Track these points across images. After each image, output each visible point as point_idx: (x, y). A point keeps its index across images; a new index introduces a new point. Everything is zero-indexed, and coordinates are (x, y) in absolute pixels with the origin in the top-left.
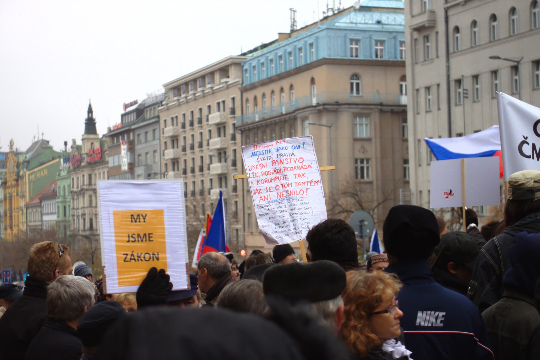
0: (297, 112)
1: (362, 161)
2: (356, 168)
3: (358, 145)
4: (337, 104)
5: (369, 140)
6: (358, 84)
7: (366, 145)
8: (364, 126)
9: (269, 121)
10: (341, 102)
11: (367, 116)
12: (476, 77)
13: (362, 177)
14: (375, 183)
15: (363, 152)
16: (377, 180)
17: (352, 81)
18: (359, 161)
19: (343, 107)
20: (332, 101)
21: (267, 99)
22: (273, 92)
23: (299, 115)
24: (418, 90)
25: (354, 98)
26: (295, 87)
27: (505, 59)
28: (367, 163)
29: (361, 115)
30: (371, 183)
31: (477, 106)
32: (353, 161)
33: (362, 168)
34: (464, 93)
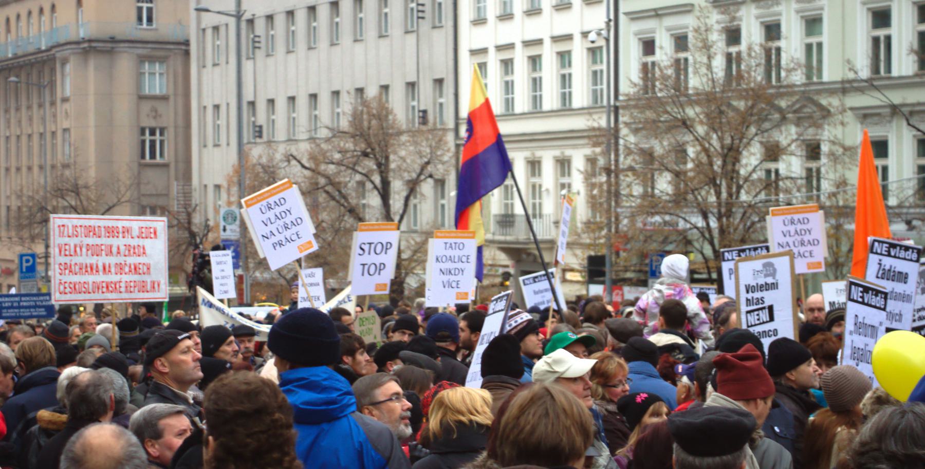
0: (53, 51)
1: (153, 133)
2: (143, 142)
3: (146, 106)
4: (113, 40)
5: (164, 98)
6: (150, 10)
7: (161, 106)
8: (157, 75)
9: (22, 59)
10: (119, 37)
11: (162, 60)
12: (270, 18)
13: (153, 156)
14: (172, 166)
15: (155, 118)
16: (176, 162)
17: (140, 4)
18: (147, 132)
19: (122, 45)
20: (105, 35)
21: (23, 22)
22: (30, 13)
23: (58, 55)
24: (204, 30)
25: (143, 31)
26: (58, 8)
27: (219, 13)
28: (161, 134)
29: (152, 59)
30: (166, 166)
31: (270, 61)
32: (136, 132)
33: (153, 143)
34: (418, 11)
